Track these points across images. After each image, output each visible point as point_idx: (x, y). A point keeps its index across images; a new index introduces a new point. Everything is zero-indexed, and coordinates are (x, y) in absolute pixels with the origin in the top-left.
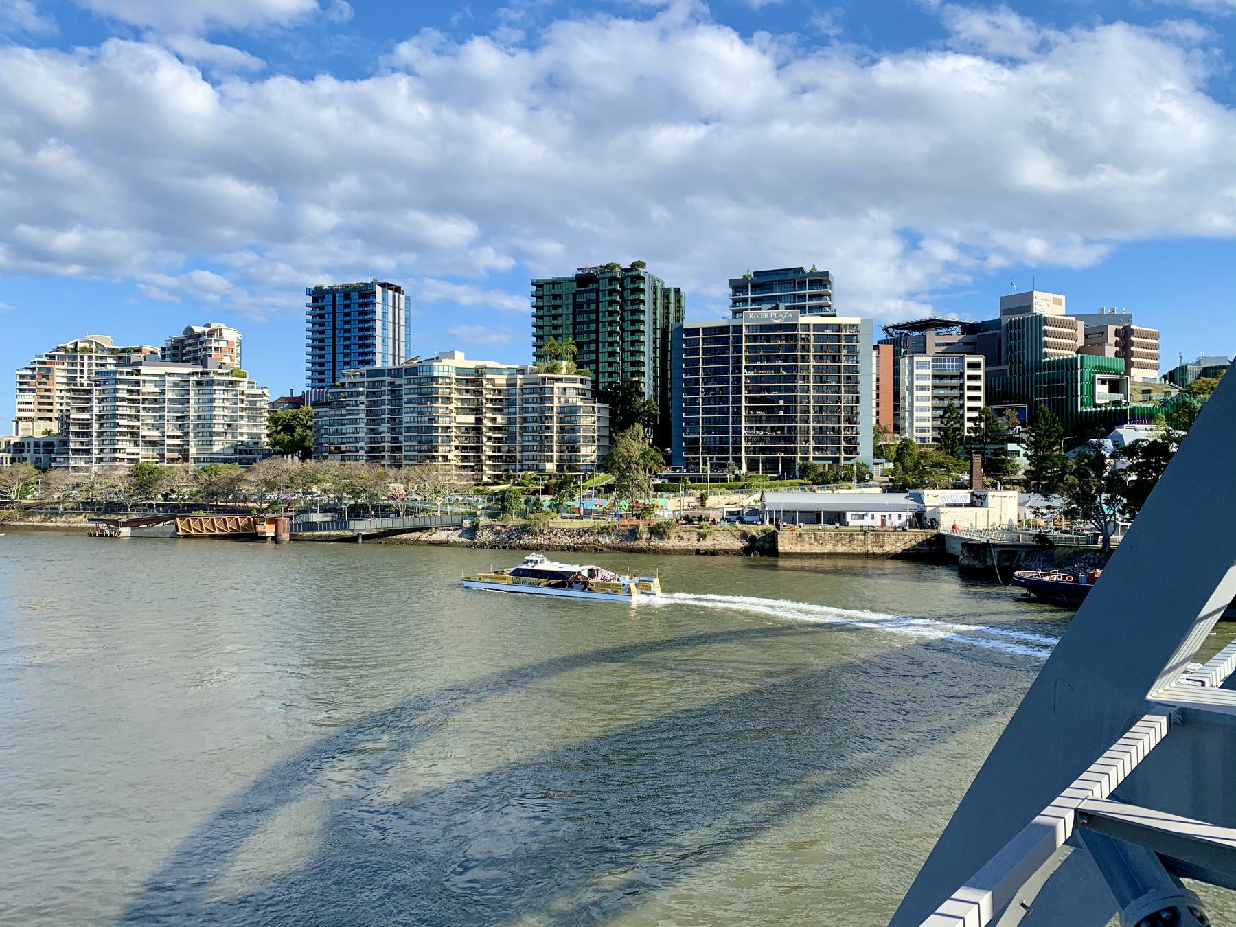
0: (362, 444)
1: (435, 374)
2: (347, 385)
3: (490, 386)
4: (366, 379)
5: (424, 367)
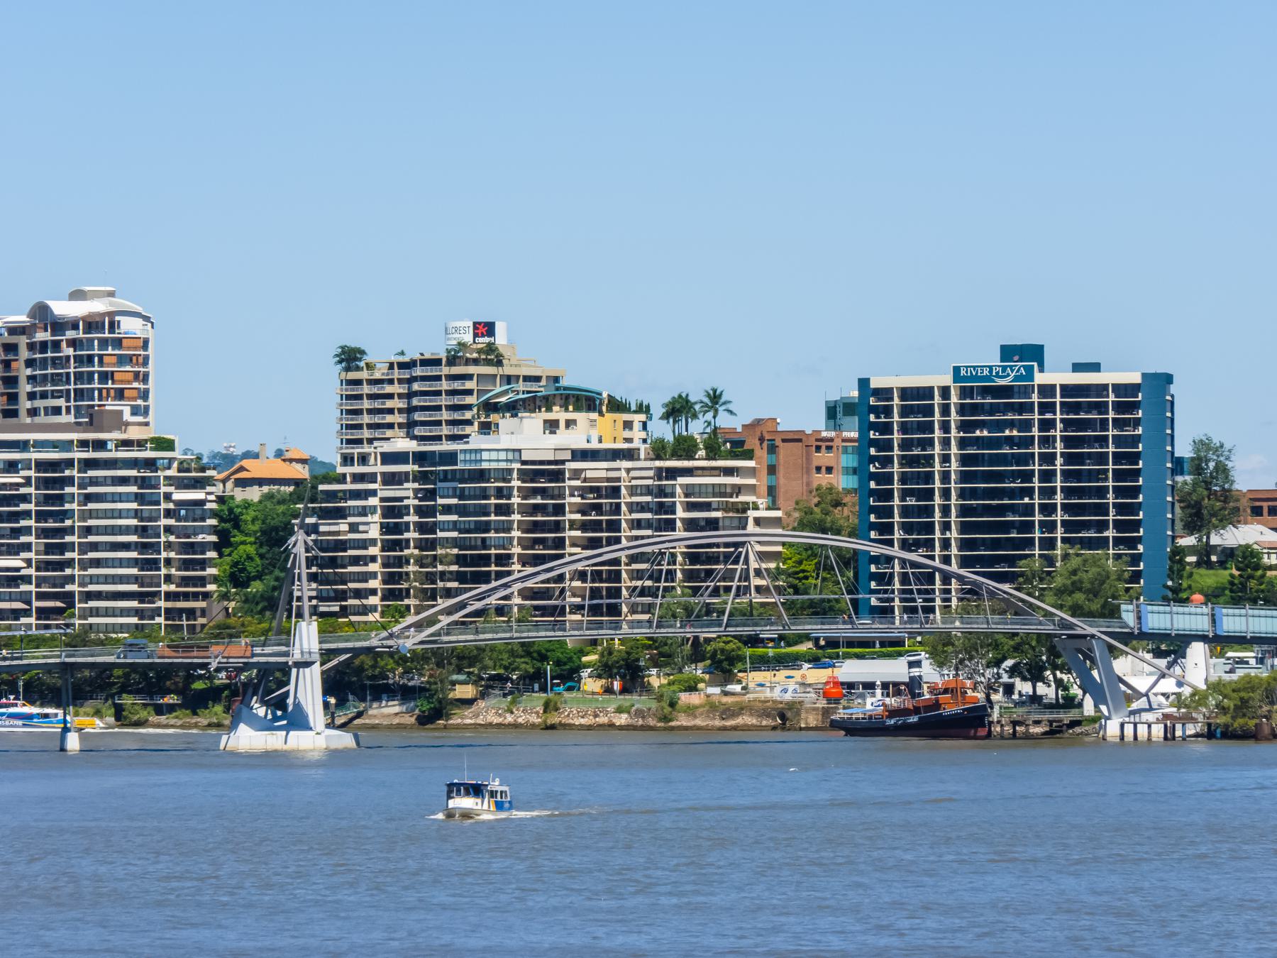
1: (485, 465)
2: (348, 479)
3: (577, 483)
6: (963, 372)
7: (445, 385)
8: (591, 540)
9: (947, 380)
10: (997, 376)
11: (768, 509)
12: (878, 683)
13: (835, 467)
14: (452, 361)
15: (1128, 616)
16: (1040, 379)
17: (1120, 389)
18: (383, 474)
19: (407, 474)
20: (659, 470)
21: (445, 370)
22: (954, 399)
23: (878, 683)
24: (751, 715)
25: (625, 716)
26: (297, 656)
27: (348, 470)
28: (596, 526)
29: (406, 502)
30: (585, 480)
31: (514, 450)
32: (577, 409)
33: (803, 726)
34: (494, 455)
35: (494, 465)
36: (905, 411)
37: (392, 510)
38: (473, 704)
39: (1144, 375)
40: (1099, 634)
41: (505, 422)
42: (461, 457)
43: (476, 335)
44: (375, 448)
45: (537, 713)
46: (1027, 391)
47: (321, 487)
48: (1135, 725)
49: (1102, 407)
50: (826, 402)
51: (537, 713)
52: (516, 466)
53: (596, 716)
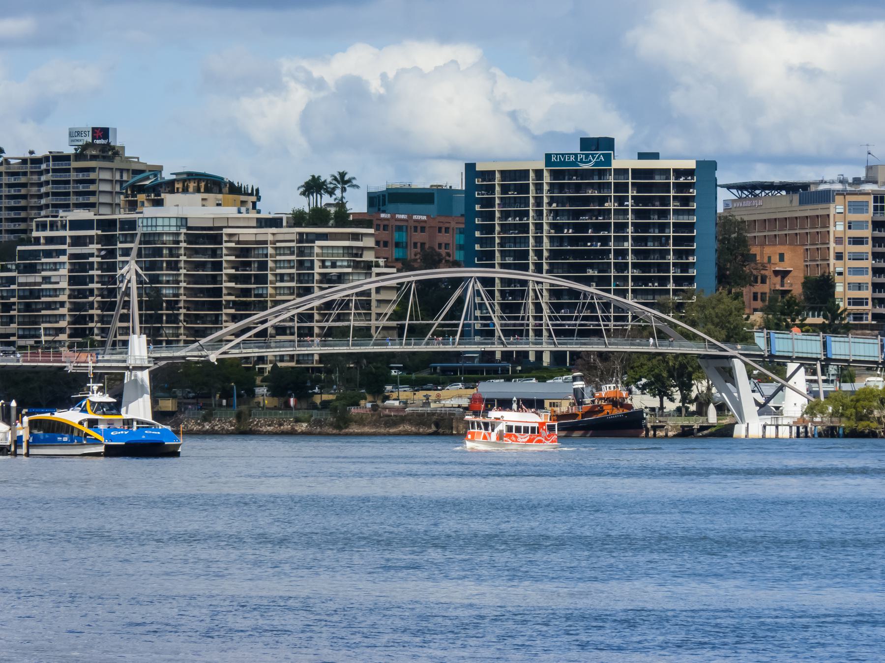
0: (63, 324)
1: (159, 230)
2: (42, 241)
3: (233, 245)
4: (68, 233)
5: (145, 221)
6: (553, 159)
7: (73, 176)
8: (242, 289)
9: (541, 165)
10: (581, 161)
11: (386, 266)
12: (515, 399)
13: (390, 241)
14: (79, 157)
15: (760, 340)
16: (616, 164)
17: (679, 173)
18: (71, 237)
19: (91, 237)
20: (301, 234)
21: (74, 164)
22: (547, 178)
23: (515, 399)
24: (411, 424)
25: (305, 425)
26: (131, 362)
27: (41, 234)
28: (246, 279)
29: (91, 259)
30: (238, 242)
31: (182, 218)
32: (207, 190)
33: (454, 432)
34: (166, 222)
35: (166, 229)
36: (505, 189)
37: (80, 265)
38: (173, 415)
39: (697, 162)
40: (739, 356)
41: (167, 197)
42: (140, 223)
43: (94, 138)
44: (61, 217)
45: (230, 422)
46: (602, 173)
47: (19, 248)
48: (777, 427)
49: (666, 187)
50: (368, 193)
51: (230, 422)
52: (183, 231)
53: (281, 425)
